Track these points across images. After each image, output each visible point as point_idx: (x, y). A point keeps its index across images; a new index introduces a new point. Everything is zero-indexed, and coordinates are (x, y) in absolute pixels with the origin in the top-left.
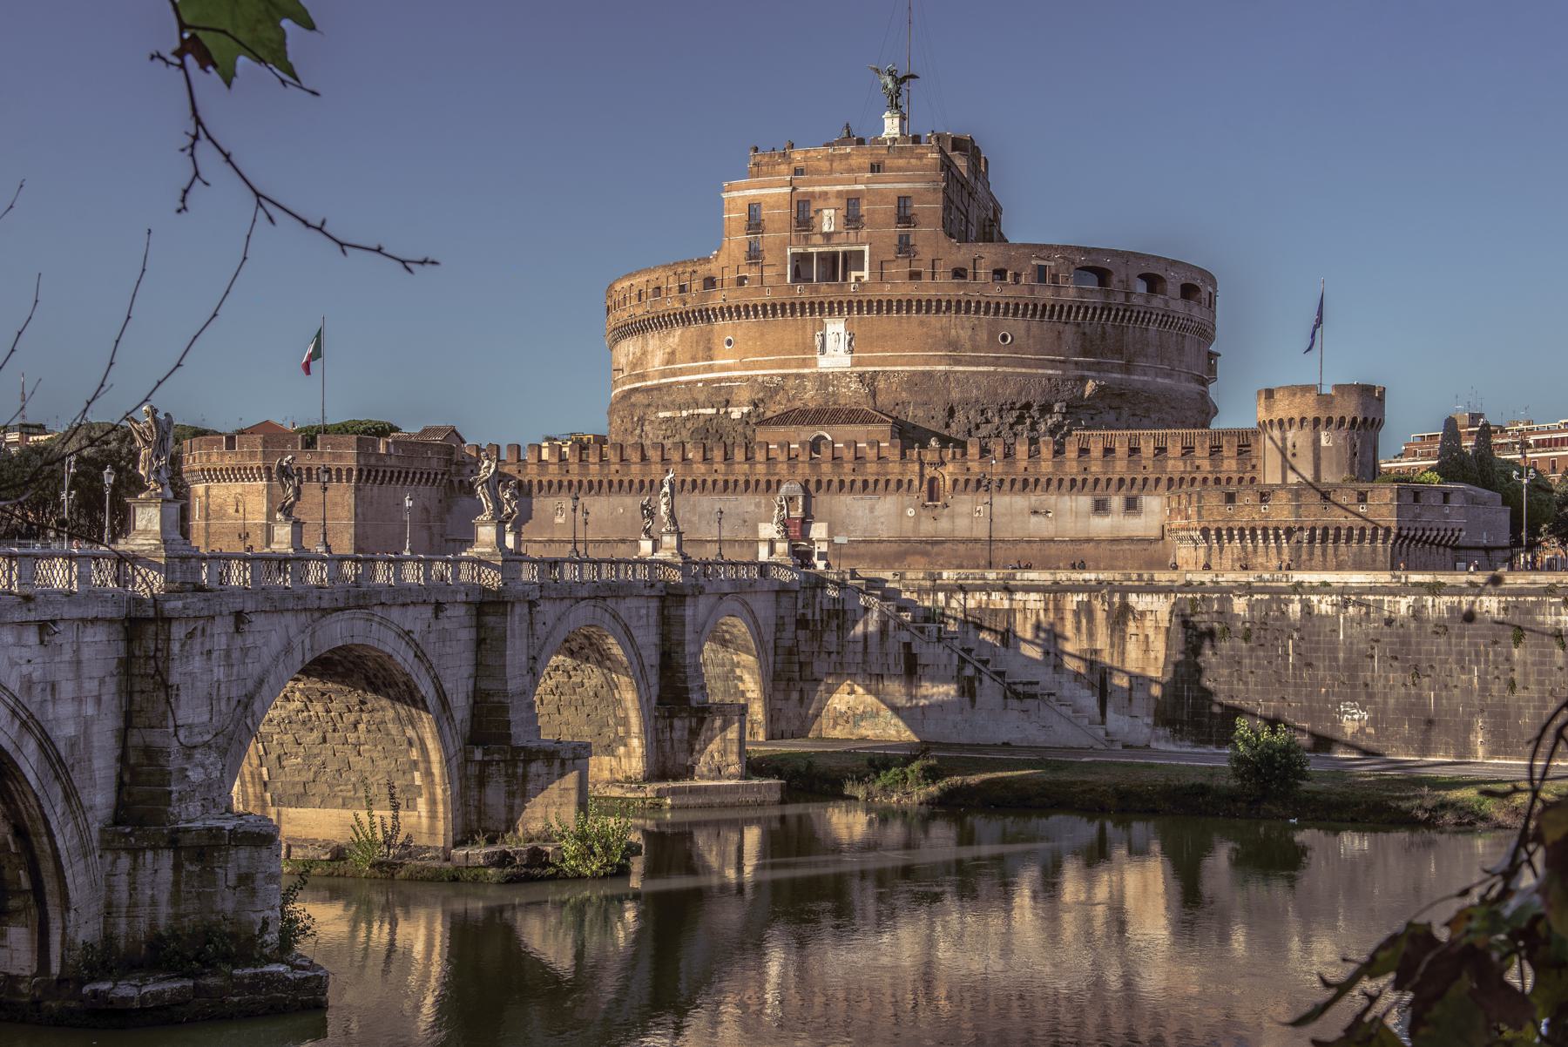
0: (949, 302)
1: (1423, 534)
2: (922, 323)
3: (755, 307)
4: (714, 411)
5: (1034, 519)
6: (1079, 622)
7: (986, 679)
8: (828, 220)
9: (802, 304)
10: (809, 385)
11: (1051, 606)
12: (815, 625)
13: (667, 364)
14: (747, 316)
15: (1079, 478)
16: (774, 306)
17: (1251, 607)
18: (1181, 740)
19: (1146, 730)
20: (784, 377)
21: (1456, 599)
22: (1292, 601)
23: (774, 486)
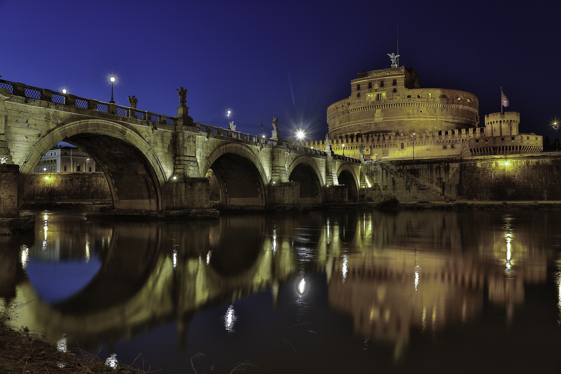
1: (530, 148)
2: (400, 109)
3: (359, 108)
5: (428, 152)
6: (437, 171)
7: (413, 186)
8: (376, 86)
9: (371, 107)
10: (373, 125)
11: (429, 167)
12: (370, 174)
15: (439, 141)
16: (364, 108)
17: (482, 165)
18: (464, 199)
19: (455, 197)
21: (538, 160)
22: (493, 163)
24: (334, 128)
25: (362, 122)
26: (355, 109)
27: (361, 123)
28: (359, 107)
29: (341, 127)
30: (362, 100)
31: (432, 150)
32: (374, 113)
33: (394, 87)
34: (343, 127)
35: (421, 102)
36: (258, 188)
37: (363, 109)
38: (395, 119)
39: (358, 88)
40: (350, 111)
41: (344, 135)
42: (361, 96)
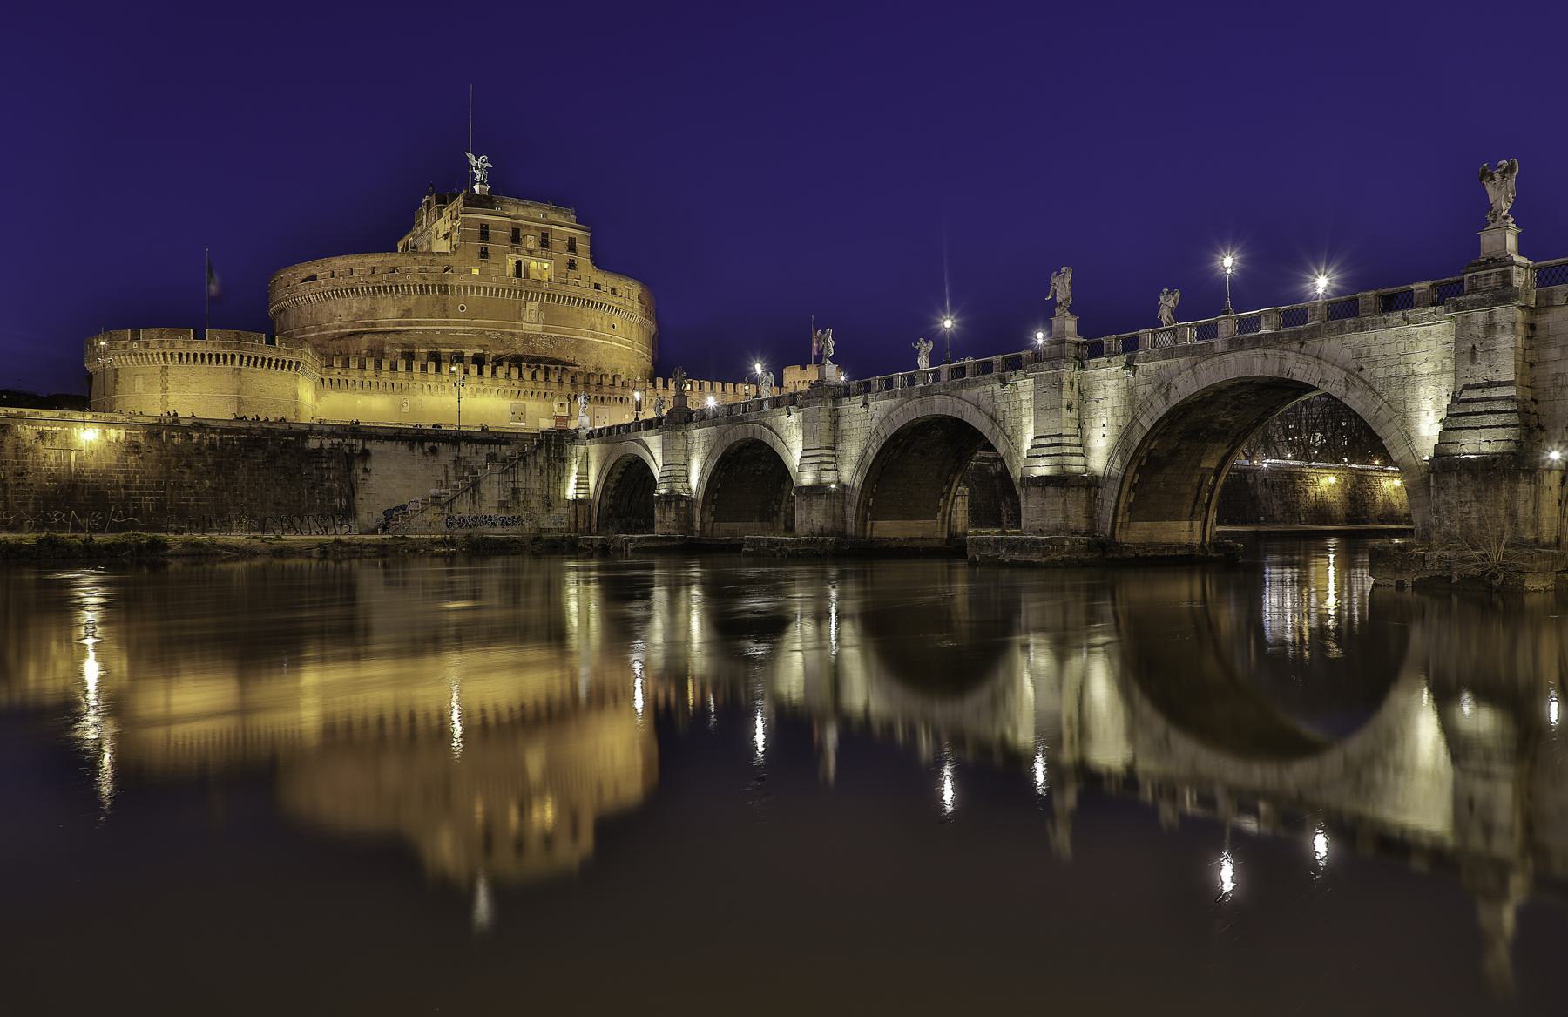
2: (579, 312)
3: (485, 288)
4: (452, 350)
8: (531, 242)
10: (518, 340)
16: (497, 290)
20: (502, 333)
23: (549, 396)
24: (373, 325)
25: (491, 326)
26: (472, 289)
27: (488, 329)
28: (485, 284)
30: (493, 269)
32: (520, 309)
33: (570, 256)
34: (417, 328)
35: (618, 306)
36: (942, 500)
39: (482, 233)
40: (453, 290)
41: (422, 350)
42: (492, 256)
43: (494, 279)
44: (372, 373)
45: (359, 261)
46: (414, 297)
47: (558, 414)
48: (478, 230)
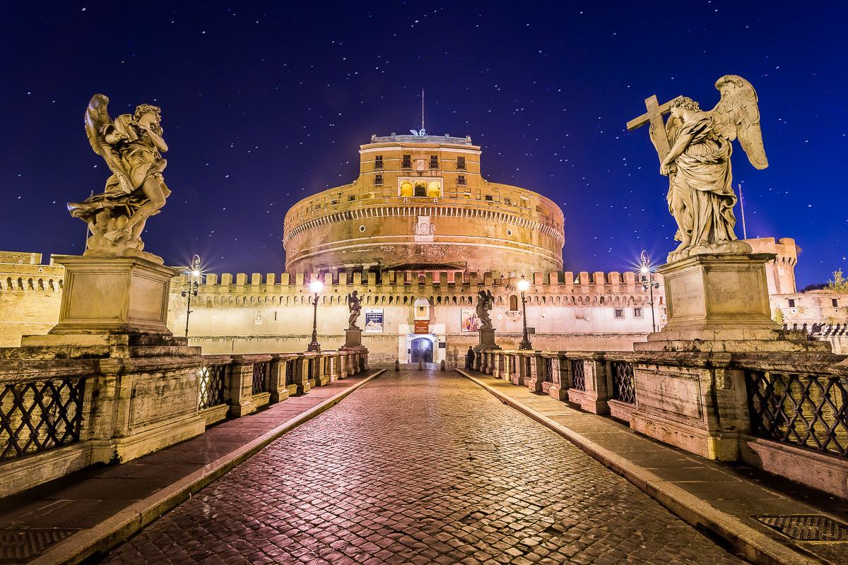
0: (485, 213)
2: (470, 221)
3: (379, 209)
8: (420, 164)
9: (407, 208)
10: (410, 251)
13: (323, 243)
14: (375, 214)
16: (390, 209)
20: (396, 246)
23: (409, 301)
25: (385, 241)
26: (369, 210)
28: (379, 205)
29: (327, 250)
30: (386, 192)
31: (588, 319)
37: (388, 212)
38: (459, 241)
40: (355, 217)
42: (385, 180)
43: (387, 200)
44: (227, 289)
45: (301, 205)
46: (331, 225)
47: (417, 318)
48: (374, 161)
